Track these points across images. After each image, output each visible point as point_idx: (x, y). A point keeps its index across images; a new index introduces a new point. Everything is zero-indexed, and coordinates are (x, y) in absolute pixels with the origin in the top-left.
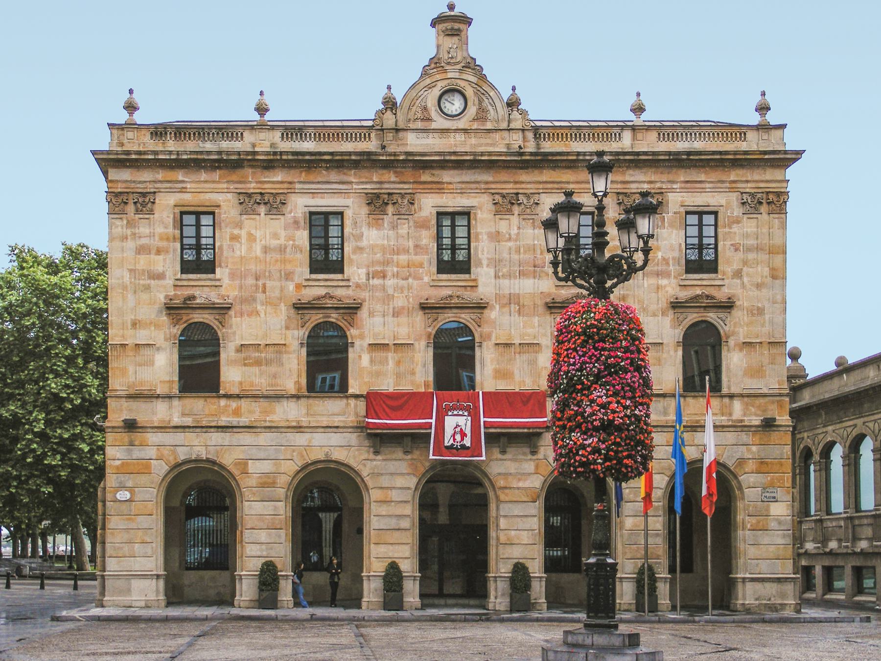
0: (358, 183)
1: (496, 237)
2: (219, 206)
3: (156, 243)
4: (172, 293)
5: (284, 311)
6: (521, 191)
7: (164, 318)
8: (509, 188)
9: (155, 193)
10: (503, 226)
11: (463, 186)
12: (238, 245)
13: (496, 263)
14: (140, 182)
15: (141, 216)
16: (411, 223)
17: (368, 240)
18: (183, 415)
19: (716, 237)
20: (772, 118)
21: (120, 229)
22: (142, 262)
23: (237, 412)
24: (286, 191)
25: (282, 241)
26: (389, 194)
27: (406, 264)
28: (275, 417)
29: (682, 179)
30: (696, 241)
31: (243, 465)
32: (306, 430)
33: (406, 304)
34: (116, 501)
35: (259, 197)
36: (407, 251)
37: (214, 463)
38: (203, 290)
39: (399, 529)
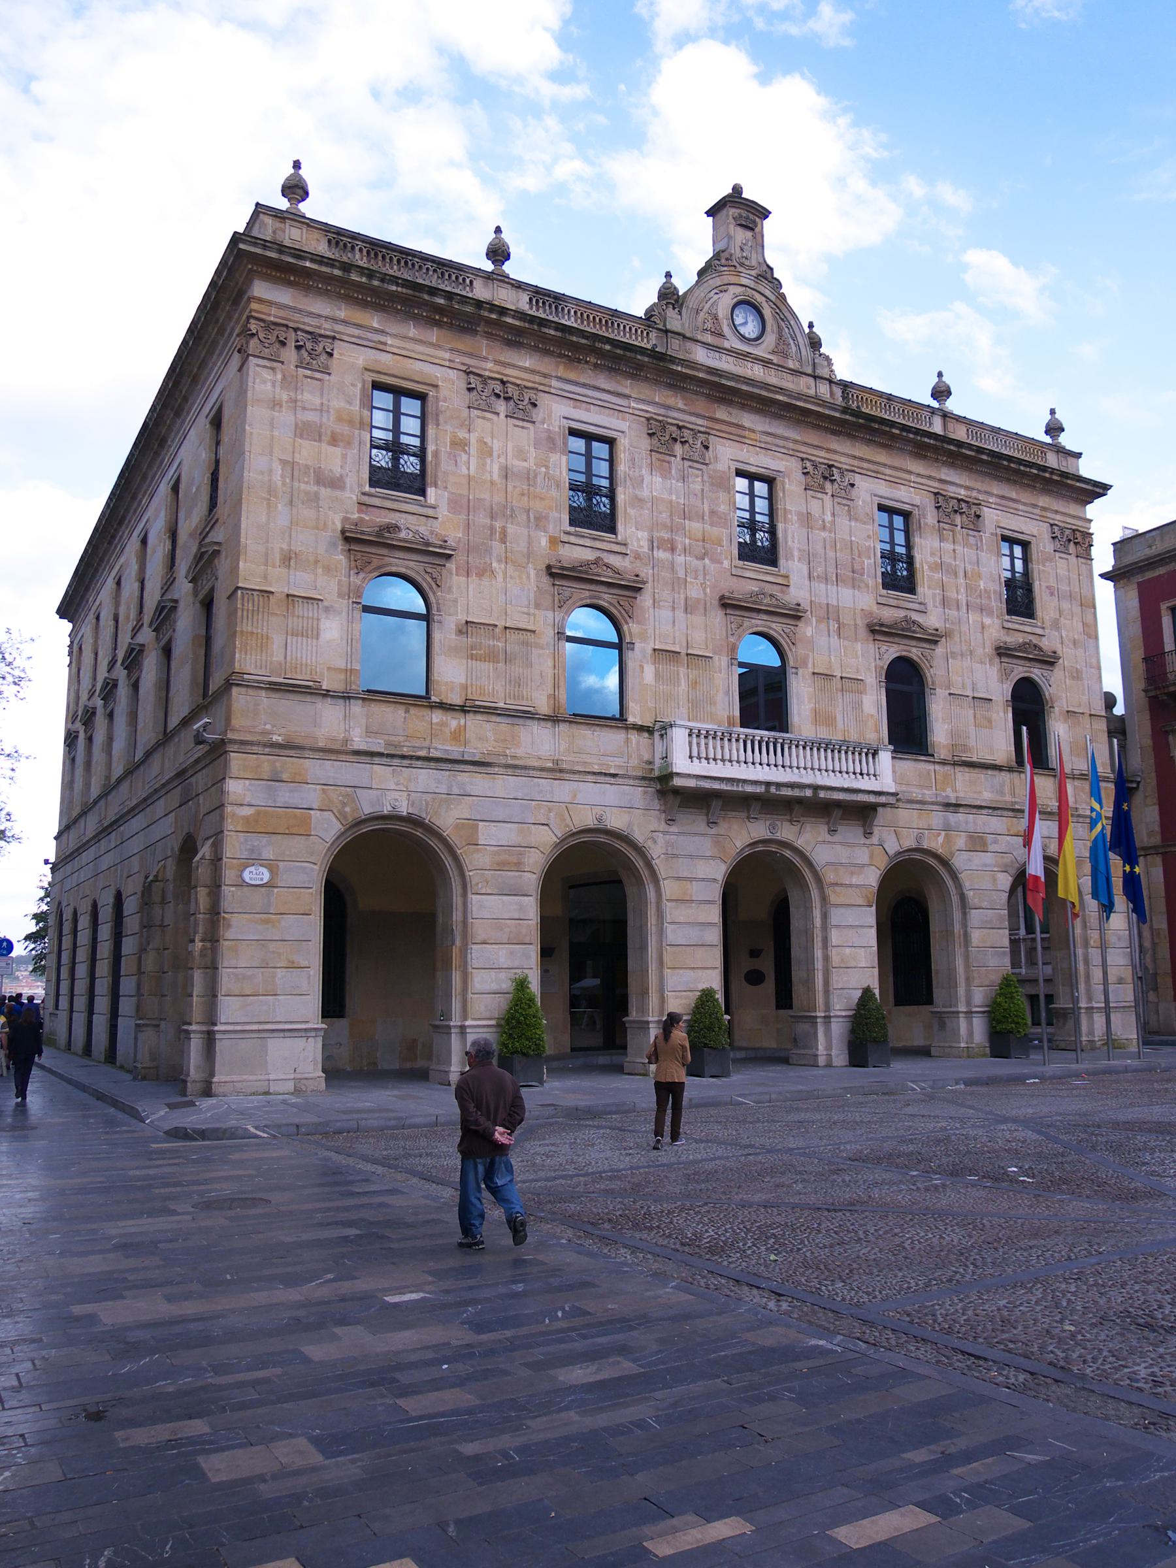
1: (807, 520)
2: (436, 386)
3: (330, 423)
4: (356, 516)
5: (533, 579)
7: (340, 558)
8: (821, 456)
9: (334, 338)
10: (815, 507)
11: (769, 439)
12: (464, 457)
13: (809, 558)
15: (308, 373)
17: (649, 489)
18: (369, 732)
21: (269, 386)
22: (305, 453)
24: (541, 388)
25: (531, 463)
26: (680, 428)
28: (520, 752)
31: (470, 826)
33: (702, 596)
34: (242, 884)
35: (498, 389)
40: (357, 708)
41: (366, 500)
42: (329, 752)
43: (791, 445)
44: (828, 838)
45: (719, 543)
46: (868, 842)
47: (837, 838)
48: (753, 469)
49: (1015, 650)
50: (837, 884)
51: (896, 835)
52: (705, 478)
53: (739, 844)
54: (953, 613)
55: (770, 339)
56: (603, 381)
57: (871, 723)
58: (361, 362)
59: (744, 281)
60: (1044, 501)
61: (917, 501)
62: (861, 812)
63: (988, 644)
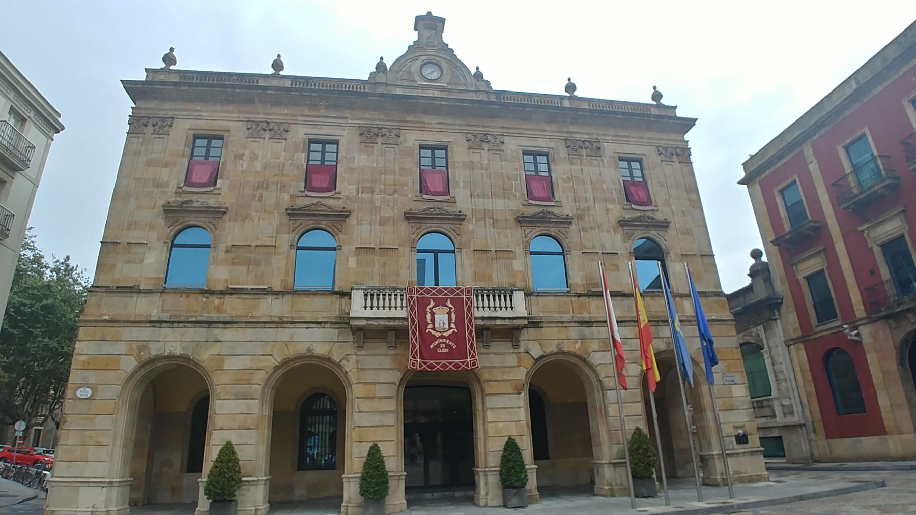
0: (352, 119)
1: (470, 166)
2: (228, 131)
5: (277, 218)
10: (476, 157)
16: (397, 151)
18: (163, 311)
19: (643, 177)
23: (218, 309)
26: (379, 128)
27: (392, 182)
32: (288, 325)
33: (392, 214)
34: (76, 398)
36: (393, 172)
39: (382, 426)
40: (156, 297)
41: (179, 190)
43: (457, 127)
45: (406, 184)
46: (516, 351)
49: (632, 221)
50: (491, 381)
51: (535, 346)
52: (397, 151)
55: (447, 78)
58: (188, 126)
59: (429, 53)
60: (649, 134)
61: (552, 145)
62: (510, 333)
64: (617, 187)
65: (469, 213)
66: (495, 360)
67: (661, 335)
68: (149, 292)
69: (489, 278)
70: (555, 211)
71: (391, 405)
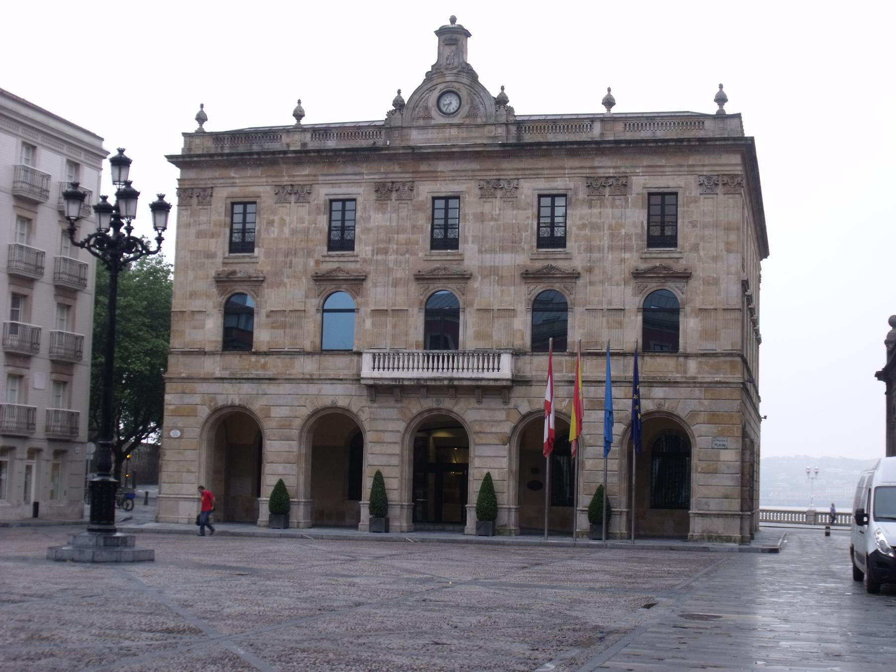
0: (368, 174)
1: (481, 218)
2: (259, 197)
4: (221, 269)
5: (305, 283)
6: (502, 177)
7: (214, 290)
8: (492, 175)
9: (212, 188)
10: (487, 208)
11: (454, 174)
13: (480, 240)
14: (201, 179)
20: (729, 109)
23: (264, 367)
25: (306, 225)
26: (393, 183)
28: (294, 371)
29: (645, 164)
30: (658, 219)
31: (268, 408)
34: (170, 438)
35: (290, 188)
37: (244, 408)
38: (243, 266)
41: (226, 261)
42: (205, 380)
44: (476, 405)
45: (417, 243)
46: (506, 407)
47: (482, 406)
48: (443, 195)
53: (415, 412)
54: (596, 255)
55: (465, 109)
56: (350, 169)
57: (519, 335)
58: (225, 195)
59: (448, 79)
60: (691, 161)
61: (571, 185)
62: (500, 391)
63: (627, 271)
64: (639, 231)
65: (476, 273)
66: (485, 415)
67: (652, 395)
68: (212, 353)
69: (491, 336)
70: (561, 264)
71: (397, 449)
